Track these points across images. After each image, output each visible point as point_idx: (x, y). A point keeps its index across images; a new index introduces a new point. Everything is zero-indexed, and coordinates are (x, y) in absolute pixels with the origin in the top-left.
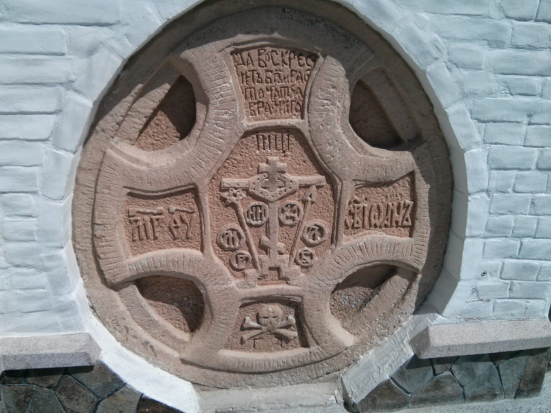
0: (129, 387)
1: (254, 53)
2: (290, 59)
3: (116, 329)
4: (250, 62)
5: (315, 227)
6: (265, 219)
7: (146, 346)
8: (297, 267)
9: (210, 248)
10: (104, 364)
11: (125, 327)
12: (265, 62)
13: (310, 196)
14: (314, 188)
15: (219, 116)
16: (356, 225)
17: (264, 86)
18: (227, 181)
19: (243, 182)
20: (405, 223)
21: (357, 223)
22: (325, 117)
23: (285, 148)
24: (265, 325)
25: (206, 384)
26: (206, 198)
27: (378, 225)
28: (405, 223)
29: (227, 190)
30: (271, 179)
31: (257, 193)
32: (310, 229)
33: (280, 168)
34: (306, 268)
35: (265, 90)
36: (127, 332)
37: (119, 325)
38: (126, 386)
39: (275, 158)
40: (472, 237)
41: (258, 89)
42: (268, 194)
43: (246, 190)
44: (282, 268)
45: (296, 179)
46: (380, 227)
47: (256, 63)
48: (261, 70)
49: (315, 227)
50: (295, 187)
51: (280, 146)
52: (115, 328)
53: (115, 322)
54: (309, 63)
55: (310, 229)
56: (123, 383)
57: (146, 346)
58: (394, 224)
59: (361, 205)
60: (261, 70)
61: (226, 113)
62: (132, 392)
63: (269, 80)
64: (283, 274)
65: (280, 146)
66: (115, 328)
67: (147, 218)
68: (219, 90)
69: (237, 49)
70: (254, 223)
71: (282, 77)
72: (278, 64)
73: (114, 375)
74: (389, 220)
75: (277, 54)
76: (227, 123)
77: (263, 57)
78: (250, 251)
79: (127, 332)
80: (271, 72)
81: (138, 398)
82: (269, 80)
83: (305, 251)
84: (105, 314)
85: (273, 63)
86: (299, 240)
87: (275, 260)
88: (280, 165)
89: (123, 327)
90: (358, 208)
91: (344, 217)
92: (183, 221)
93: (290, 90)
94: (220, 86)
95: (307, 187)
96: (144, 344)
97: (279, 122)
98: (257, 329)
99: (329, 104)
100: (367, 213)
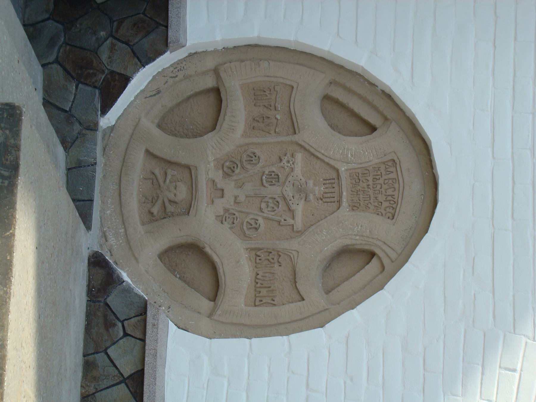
0: (141, 69)
2: (390, 200)
3: (174, 69)
4: (388, 173)
5: (258, 224)
6: (266, 185)
7: (156, 91)
10: (165, 53)
11: (177, 76)
12: (387, 183)
13: (285, 220)
14: (291, 222)
15: (350, 151)
16: (258, 258)
17: (371, 183)
18: (299, 156)
20: (258, 299)
21: (260, 260)
22: (348, 227)
23: (324, 200)
25: (111, 138)
27: (258, 277)
28: (258, 299)
29: (292, 156)
32: (256, 221)
33: (309, 196)
35: (368, 183)
36: (172, 77)
37: (178, 71)
38: (142, 68)
40: (251, 345)
41: (369, 178)
43: (292, 170)
45: (299, 209)
46: (256, 278)
47: (386, 178)
49: (258, 224)
50: (293, 207)
51: (326, 195)
52: (176, 68)
53: (182, 69)
54: (387, 214)
55: (256, 221)
56: (145, 66)
57: (156, 91)
60: (381, 181)
61: (352, 155)
62: (136, 71)
63: (375, 186)
65: (326, 195)
66: (176, 68)
68: (368, 151)
69: (396, 164)
71: (377, 196)
72: (386, 192)
73: (154, 60)
74: (262, 286)
75: (393, 191)
76: (345, 156)
77: (391, 182)
79: (172, 77)
80: (381, 188)
81: (129, 74)
82: (375, 186)
83: (237, 218)
84: (190, 62)
85: (387, 189)
89: (177, 74)
90: (273, 259)
93: (367, 202)
94: (371, 152)
95: (293, 218)
96: (158, 89)
97: (344, 194)
99: (358, 229)
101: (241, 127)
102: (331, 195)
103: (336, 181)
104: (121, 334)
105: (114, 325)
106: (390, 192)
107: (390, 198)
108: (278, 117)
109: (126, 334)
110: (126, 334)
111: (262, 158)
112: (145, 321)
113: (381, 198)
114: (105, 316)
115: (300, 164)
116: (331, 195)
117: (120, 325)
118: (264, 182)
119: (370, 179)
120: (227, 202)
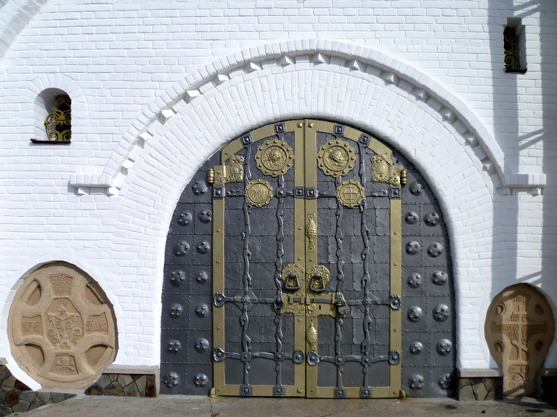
1: (56, 278)
8: (72, 344)
9: (45, 335)
18: (49, 314)
19: (54, 314)
24: (63, 364)
26: (43, 318)
28: (106, 330)
30: (62, 314)
31: (58, 317)
34: (75, 344)
39: (63, 307)
42: (61, 318)
43: (55, 316)
44: (67, 343)
45: (69, 314)
48: (58, 282)
58: (102, 330)
59: (91, 323)
60: (58, 282)
64: (68, 346)
67: (27, 324)
70: (58, 327)
78: (57, 337)
86: (72, 334)
87: (65, 340)
88: (64, 309)
91: (85, 327)
92: (37, 326)
97: (63, 297)
98: (62, 365)
100: (93, 326)
101: (40, 336)
102: (64, 302)
103: (59, 300)
104: (116, 382)
105: (113, 385)
106: (62, 279)
107: (65, 279)
108: (34, 322)
109: (117, 381)
110: (117, 381)
111: (51, 328)
112: (111, 374)
113: (65, 282)
114: (110, 388)
115: (52, 314)
116: (64, 302)
117: (113, 383)
118: (59, 327)
119: (57, 286)
120: (68, 341)
